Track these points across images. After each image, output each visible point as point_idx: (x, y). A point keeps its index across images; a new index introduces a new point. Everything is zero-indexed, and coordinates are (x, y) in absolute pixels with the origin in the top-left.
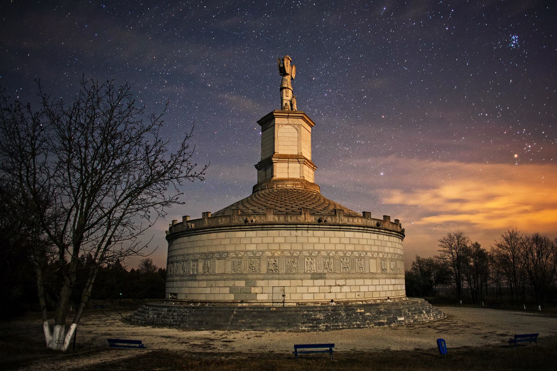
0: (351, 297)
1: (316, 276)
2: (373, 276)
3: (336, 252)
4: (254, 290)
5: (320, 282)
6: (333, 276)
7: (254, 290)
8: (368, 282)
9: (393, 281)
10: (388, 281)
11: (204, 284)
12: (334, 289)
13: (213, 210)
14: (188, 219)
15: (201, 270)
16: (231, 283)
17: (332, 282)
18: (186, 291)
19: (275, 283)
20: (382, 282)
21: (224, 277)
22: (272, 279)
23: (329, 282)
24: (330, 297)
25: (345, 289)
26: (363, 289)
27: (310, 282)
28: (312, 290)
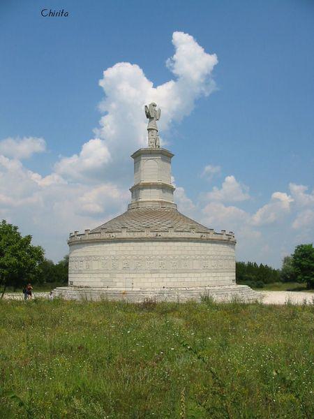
0: (178, 285)
1: (154, 271)
2: (195, 271)
3: (168, 255)
4: (115, 280)
5: (154, 275)
6: (165, 271)
7: (115, 280)
8: (191, 275)
9: (214, 275)
10: (209, 275)
11: (86, 276)
12: (165, 280)
13: (91, 228)
14: (78, 233)
15: (85, 268)
16: (101, 275)
17: (164, 275)
18: (77, 280)
19: (127, 276)
20: (204, 275)
21: (98, 272)
22: (126, 273)
23: (162, 275)
24: (162, 285)
25: (173, 280)
26: (186, 280)
27: (149, 276)
28: (150, 280)
